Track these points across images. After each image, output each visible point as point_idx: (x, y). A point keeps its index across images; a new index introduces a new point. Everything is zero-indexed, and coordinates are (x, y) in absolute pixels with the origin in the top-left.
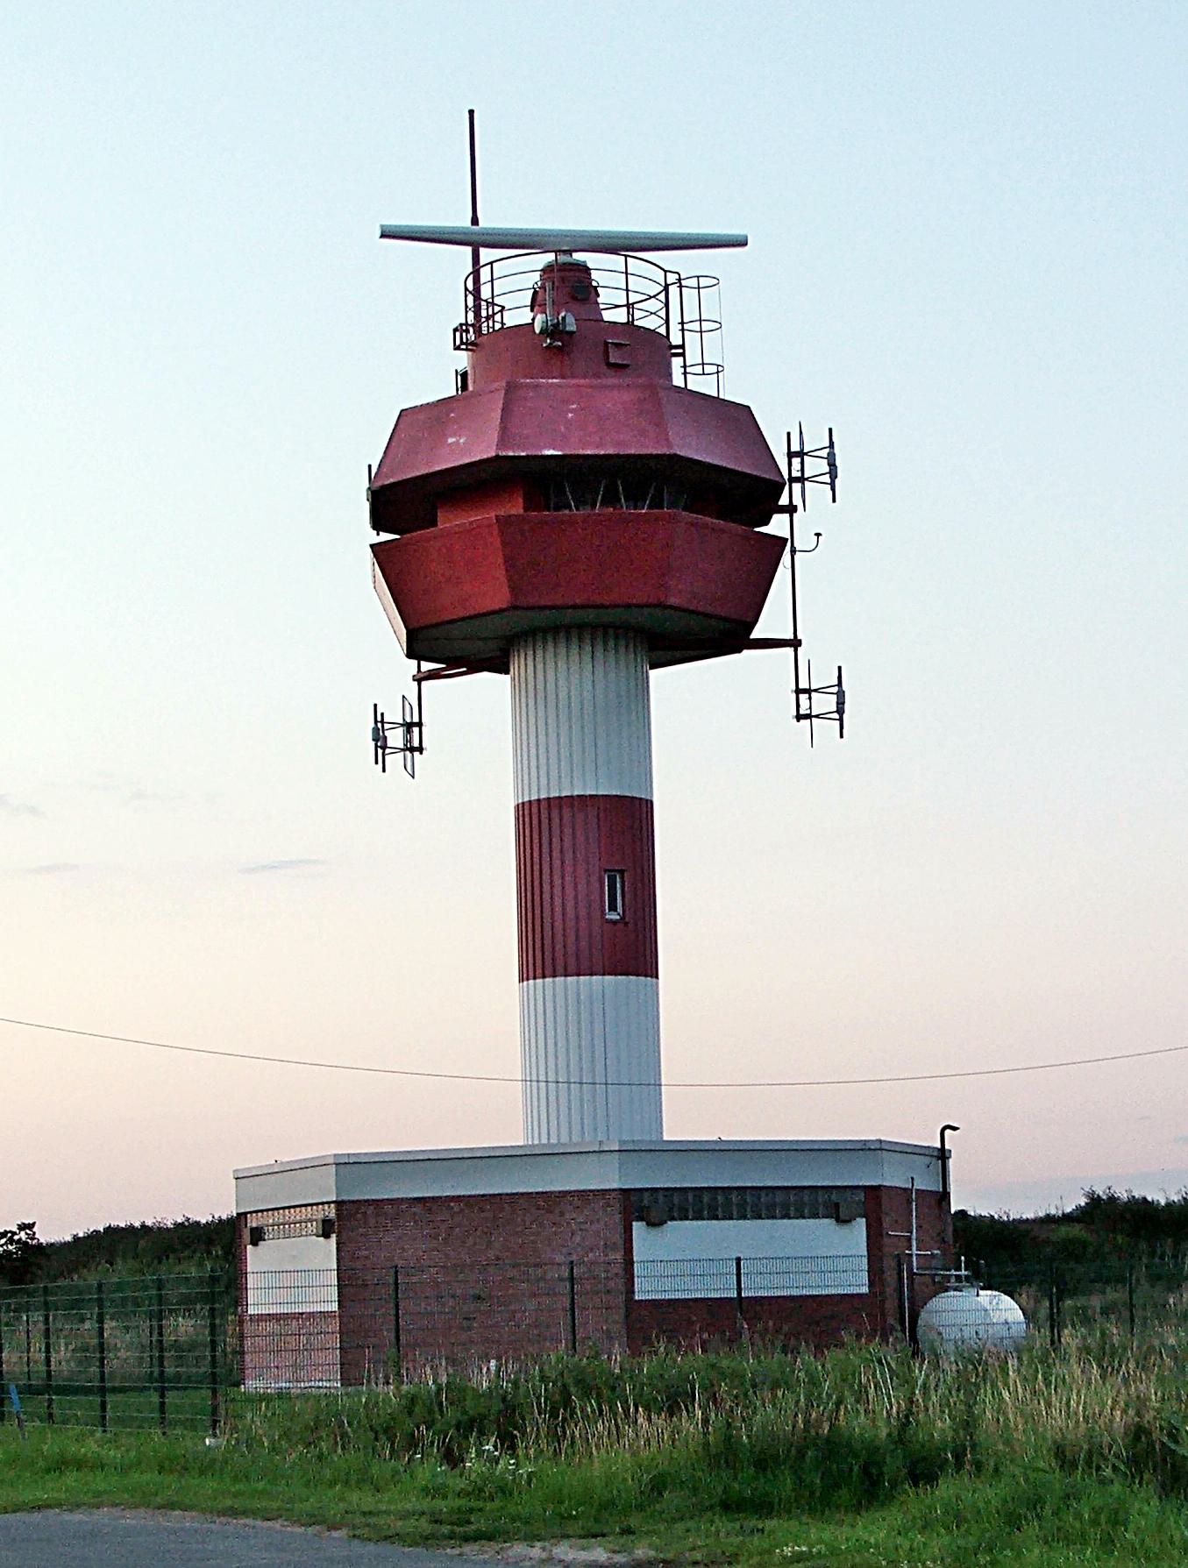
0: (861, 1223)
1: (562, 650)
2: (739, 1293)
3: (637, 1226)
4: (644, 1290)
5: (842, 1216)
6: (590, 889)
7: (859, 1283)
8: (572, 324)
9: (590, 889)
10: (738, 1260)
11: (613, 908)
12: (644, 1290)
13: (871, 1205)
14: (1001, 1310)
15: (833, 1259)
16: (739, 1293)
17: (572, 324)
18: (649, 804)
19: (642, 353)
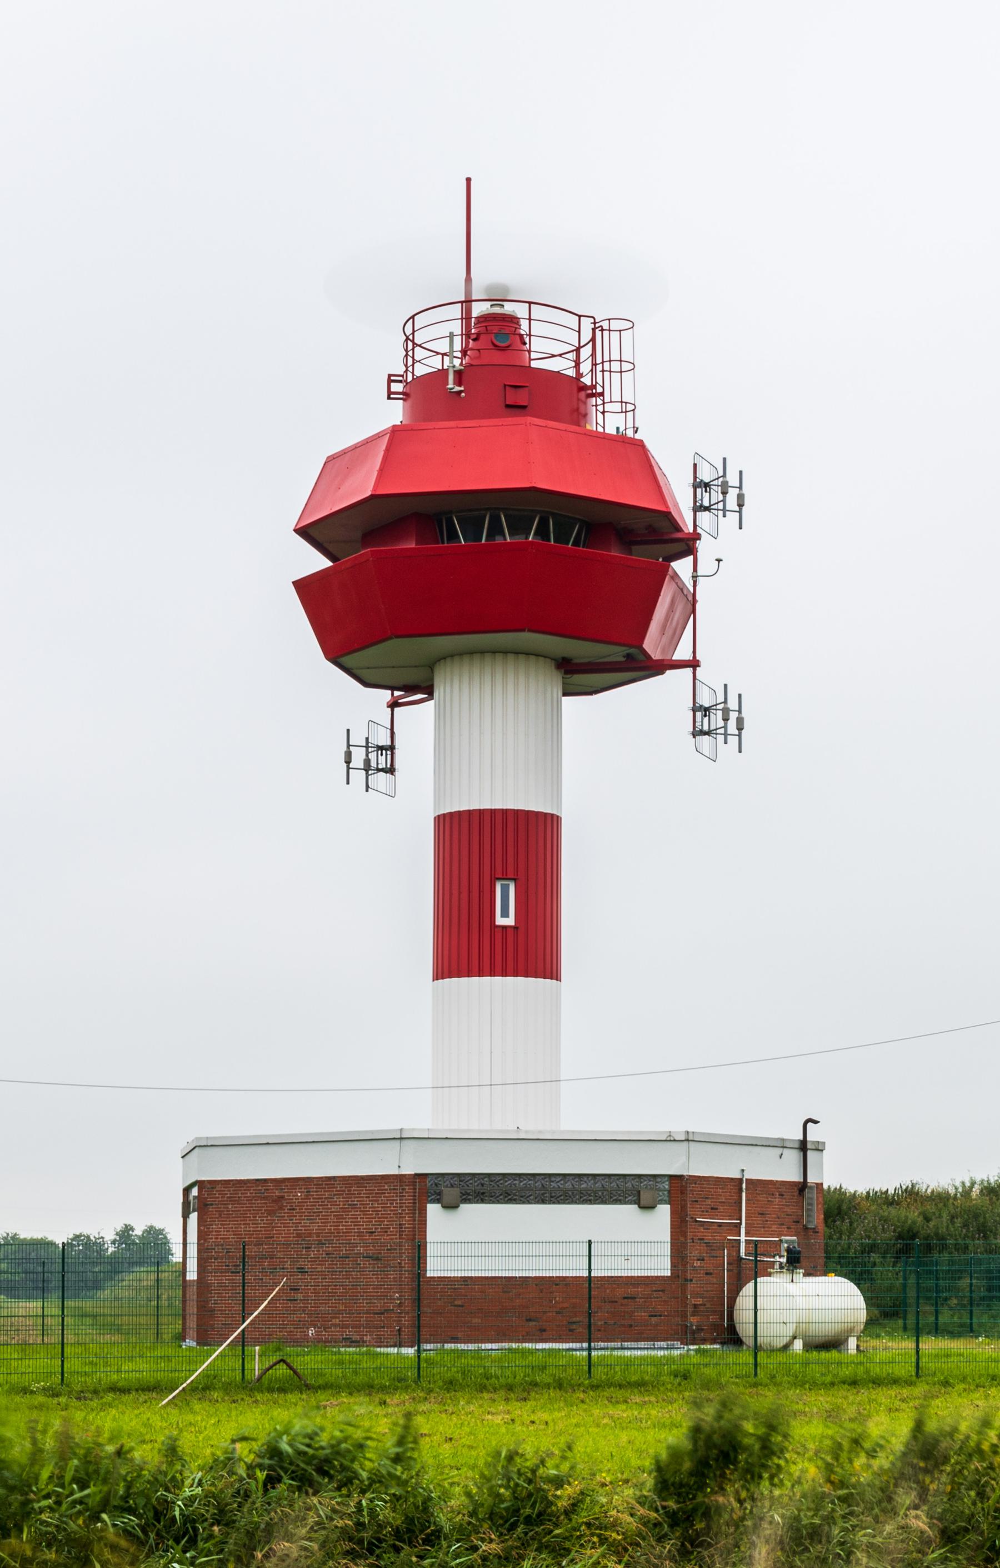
0: (664, 1211)
1: (499, 677)
2: (590, 1273)
3: (433, 1210)
4: (436, 1267)
5: (643, 1203)
6: (497, 894)
7: (661, 1266)
8: (493, 370)
9: (497, 894)
10: (590, 1242)
11: (505, 914)
12: (436, 1267)
13: (681, 1193)
14: (833, 1300)
15: (637, 1244)
16: (590, 1273)
17: (493, 370)
18: (558, 819)
19: (568, 397)
